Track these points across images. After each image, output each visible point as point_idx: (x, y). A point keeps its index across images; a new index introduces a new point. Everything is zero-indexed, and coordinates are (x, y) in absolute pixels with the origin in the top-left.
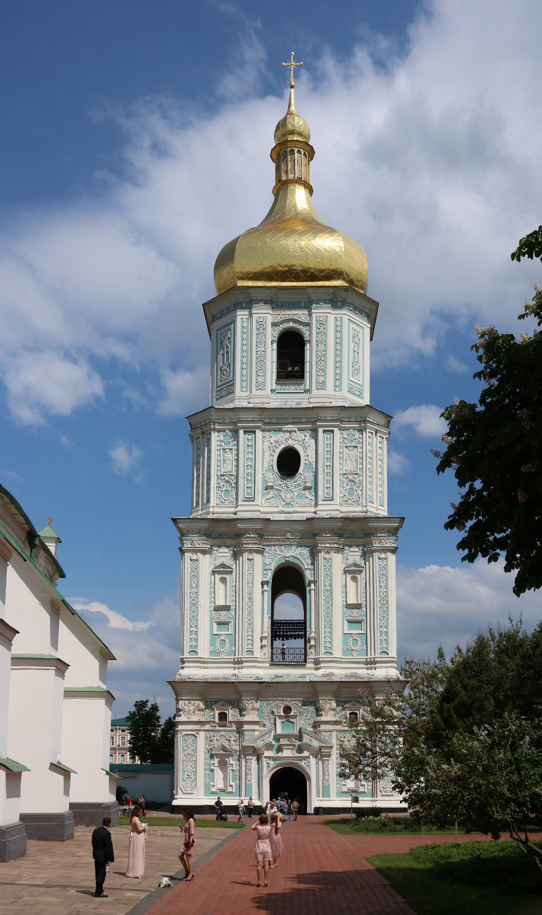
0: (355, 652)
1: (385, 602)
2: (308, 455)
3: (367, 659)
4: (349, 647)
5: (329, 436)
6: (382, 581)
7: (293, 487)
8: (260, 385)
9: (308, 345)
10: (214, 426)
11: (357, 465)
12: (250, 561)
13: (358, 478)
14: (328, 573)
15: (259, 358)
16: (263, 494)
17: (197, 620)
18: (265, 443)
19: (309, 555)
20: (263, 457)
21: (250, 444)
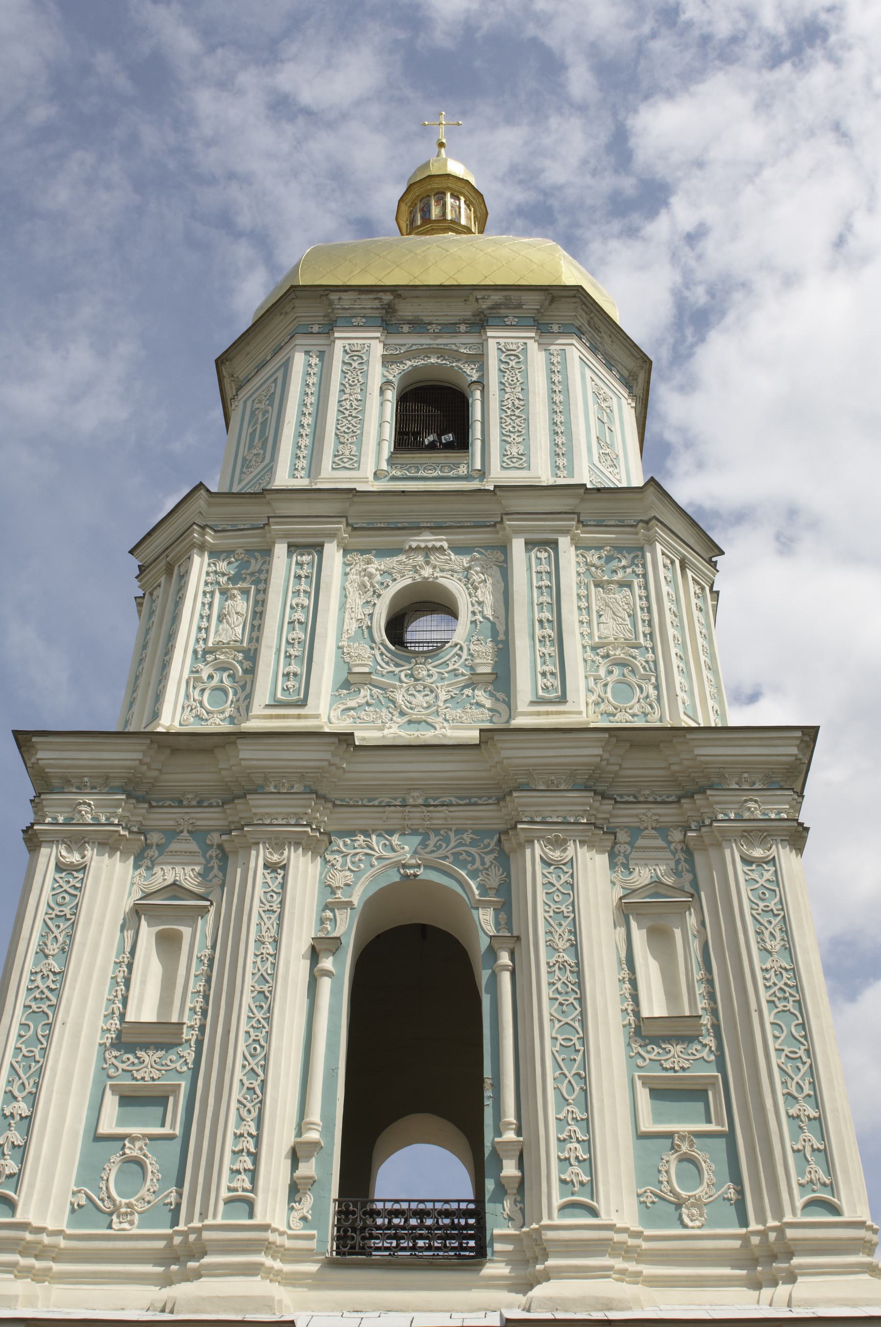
0: (694, 1211)
1: (790, 1006)
2: (480, 603)
3: (745, 1238)
4: (665, 1187)
5: (543, 555)
6: (767, 934)
7: (435, 678)
8: (345, 460)
9: (478, 394)
10: (203, 535)
11: (635, 625)
12: (274, 871)
13: (642, 655)
14: (563, 908)
15: (347, 413)
16: (336, 698)
17: (40, 1072)
18: (351, 577)
19: (488, 859)
20: (343, 607)
21: (303, 573)
